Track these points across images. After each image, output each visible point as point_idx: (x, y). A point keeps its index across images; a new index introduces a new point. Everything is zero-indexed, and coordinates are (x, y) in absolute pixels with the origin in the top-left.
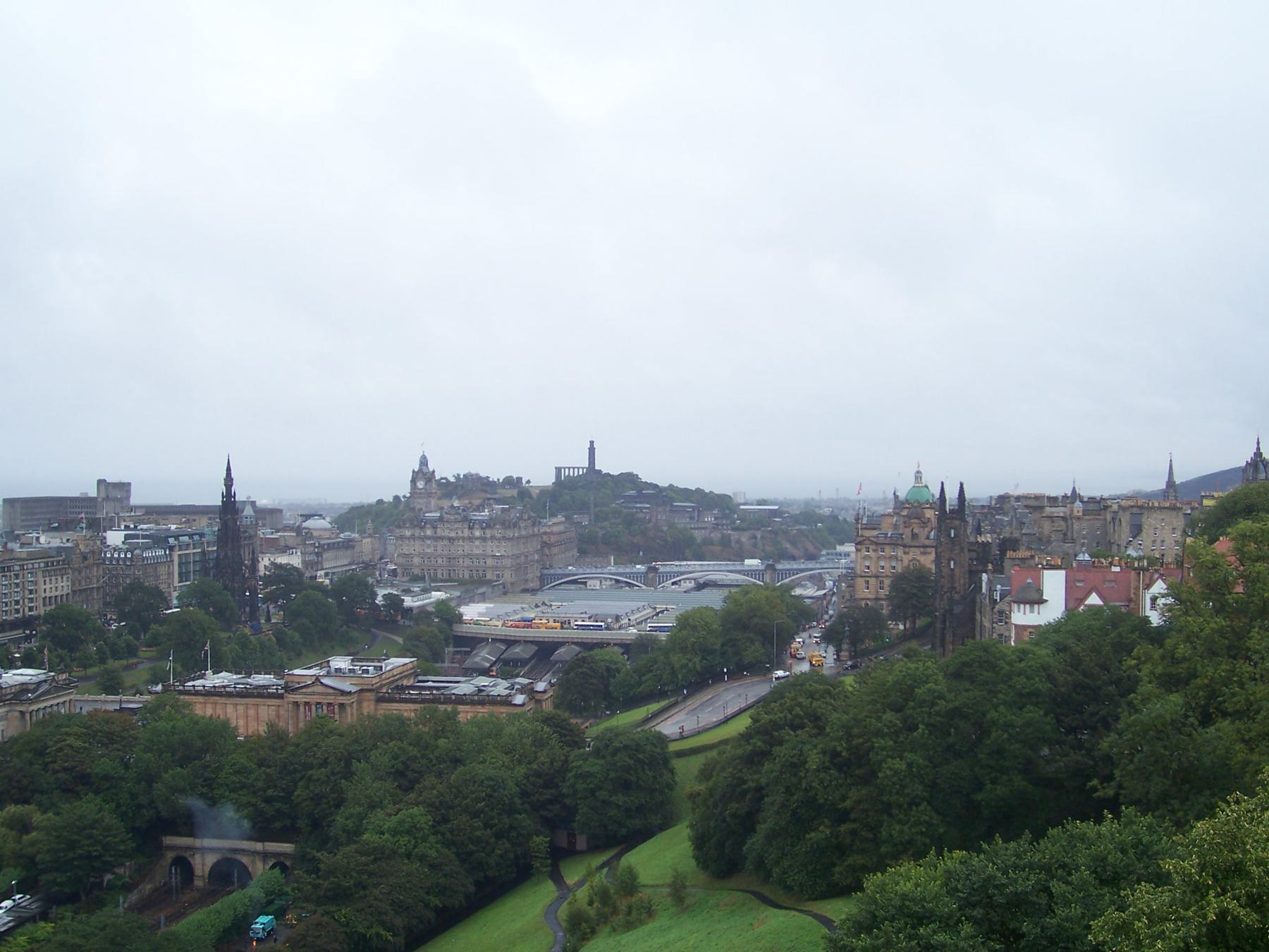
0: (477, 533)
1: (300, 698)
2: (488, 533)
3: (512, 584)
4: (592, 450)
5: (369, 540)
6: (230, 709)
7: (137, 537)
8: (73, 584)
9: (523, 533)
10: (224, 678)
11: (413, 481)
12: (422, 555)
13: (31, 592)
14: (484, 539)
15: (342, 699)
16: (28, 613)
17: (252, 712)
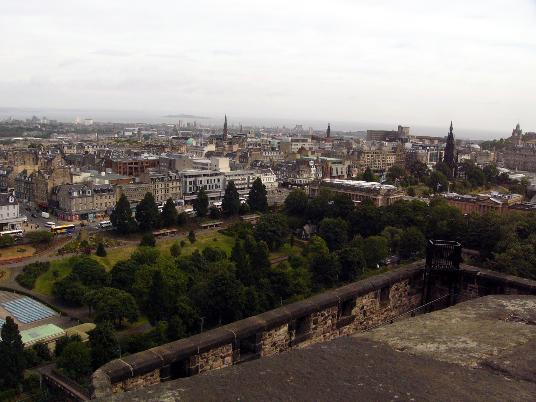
1: (481, 204)
6: (456, 205)
7: (417, 146)
10: (454, 194)
15: (496, 206)
17: (464, 207)
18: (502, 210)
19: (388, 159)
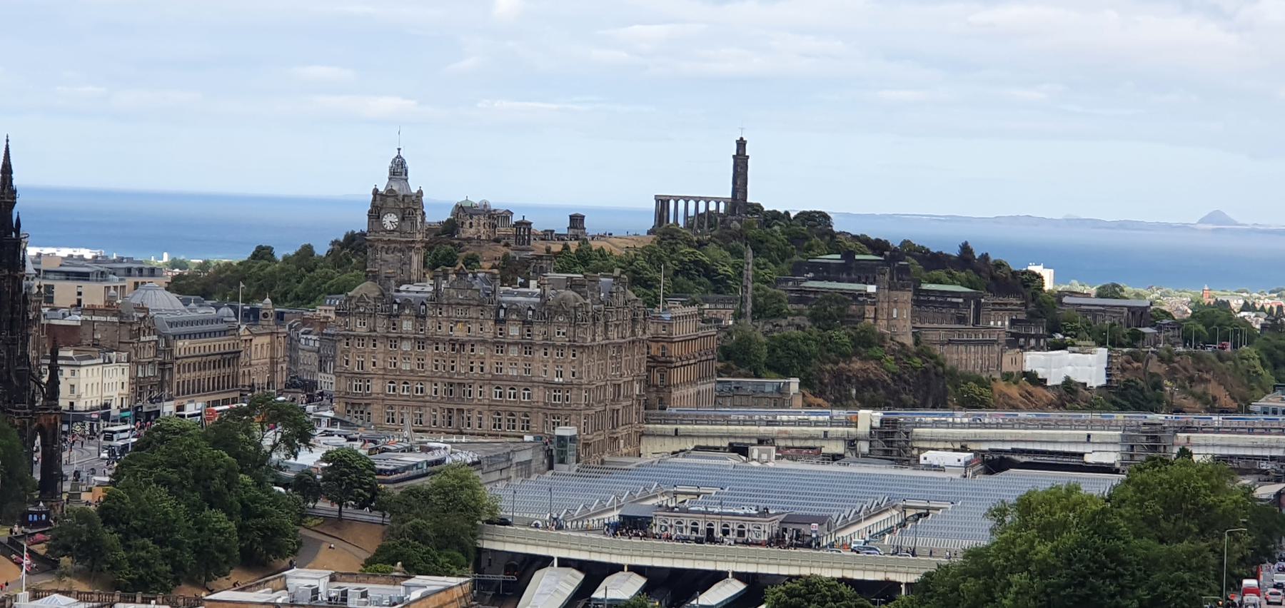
4: (741, 162)
5: (266, 340)
9: (614, 335)
11: (376, 213)
14: (528, 347)
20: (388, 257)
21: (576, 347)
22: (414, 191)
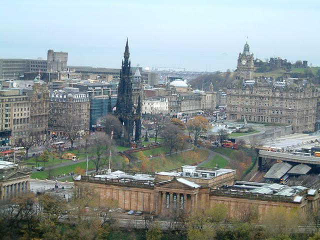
0: (278, 95)
1: (162, 189)
2: (284, 94)
3: (298, 127)
5: (211, 95)
8: (32, 112)
9: (307, 96)
11: (240, 61)
12: (243, 107)
13: (7, 115)
14: (281, 98)
15: (188, 192)
16: (4, 128)
17: (134, 196)
18: (200, 198)
19: (17, 113)
20: (243, 73)
21: (295, 99)
22: (251, 53)
